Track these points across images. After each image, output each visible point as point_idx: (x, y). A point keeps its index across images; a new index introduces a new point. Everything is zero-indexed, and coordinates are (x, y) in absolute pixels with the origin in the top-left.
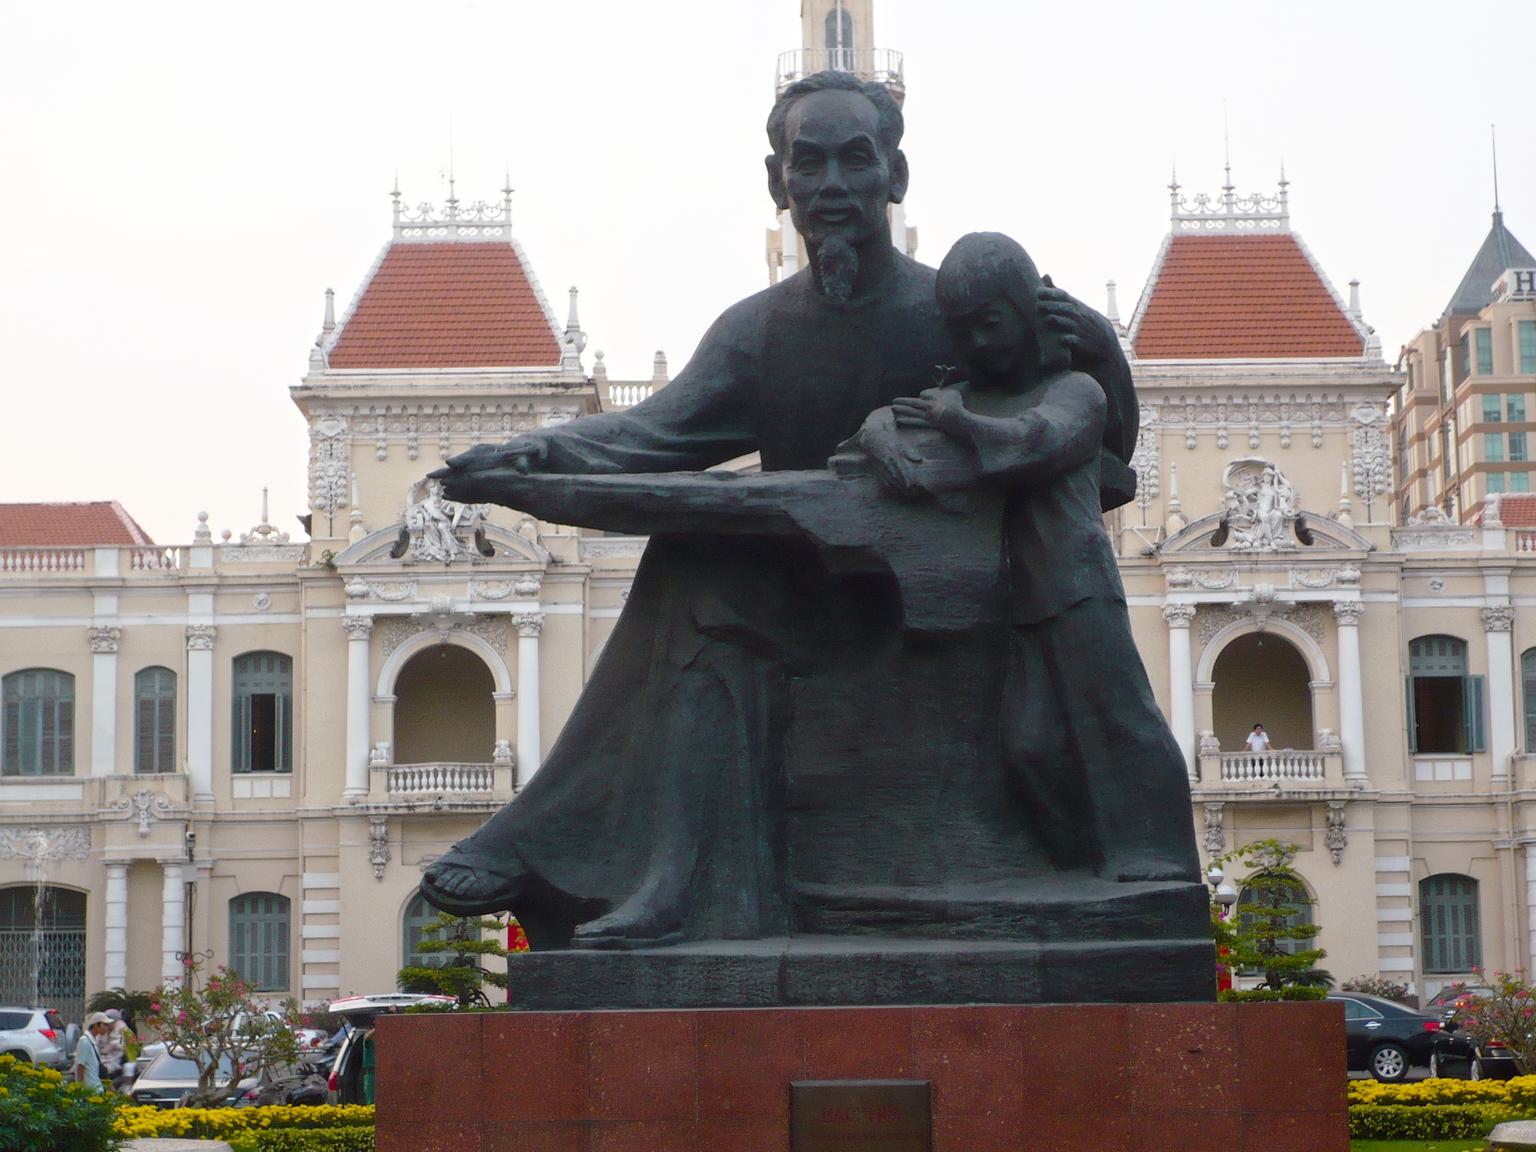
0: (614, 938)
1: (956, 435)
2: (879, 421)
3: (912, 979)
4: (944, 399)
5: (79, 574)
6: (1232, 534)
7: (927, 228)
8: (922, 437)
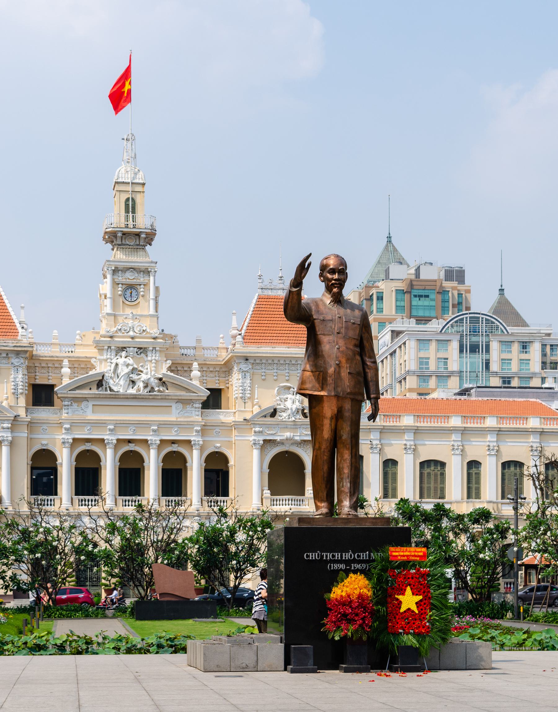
6: (278, 413)
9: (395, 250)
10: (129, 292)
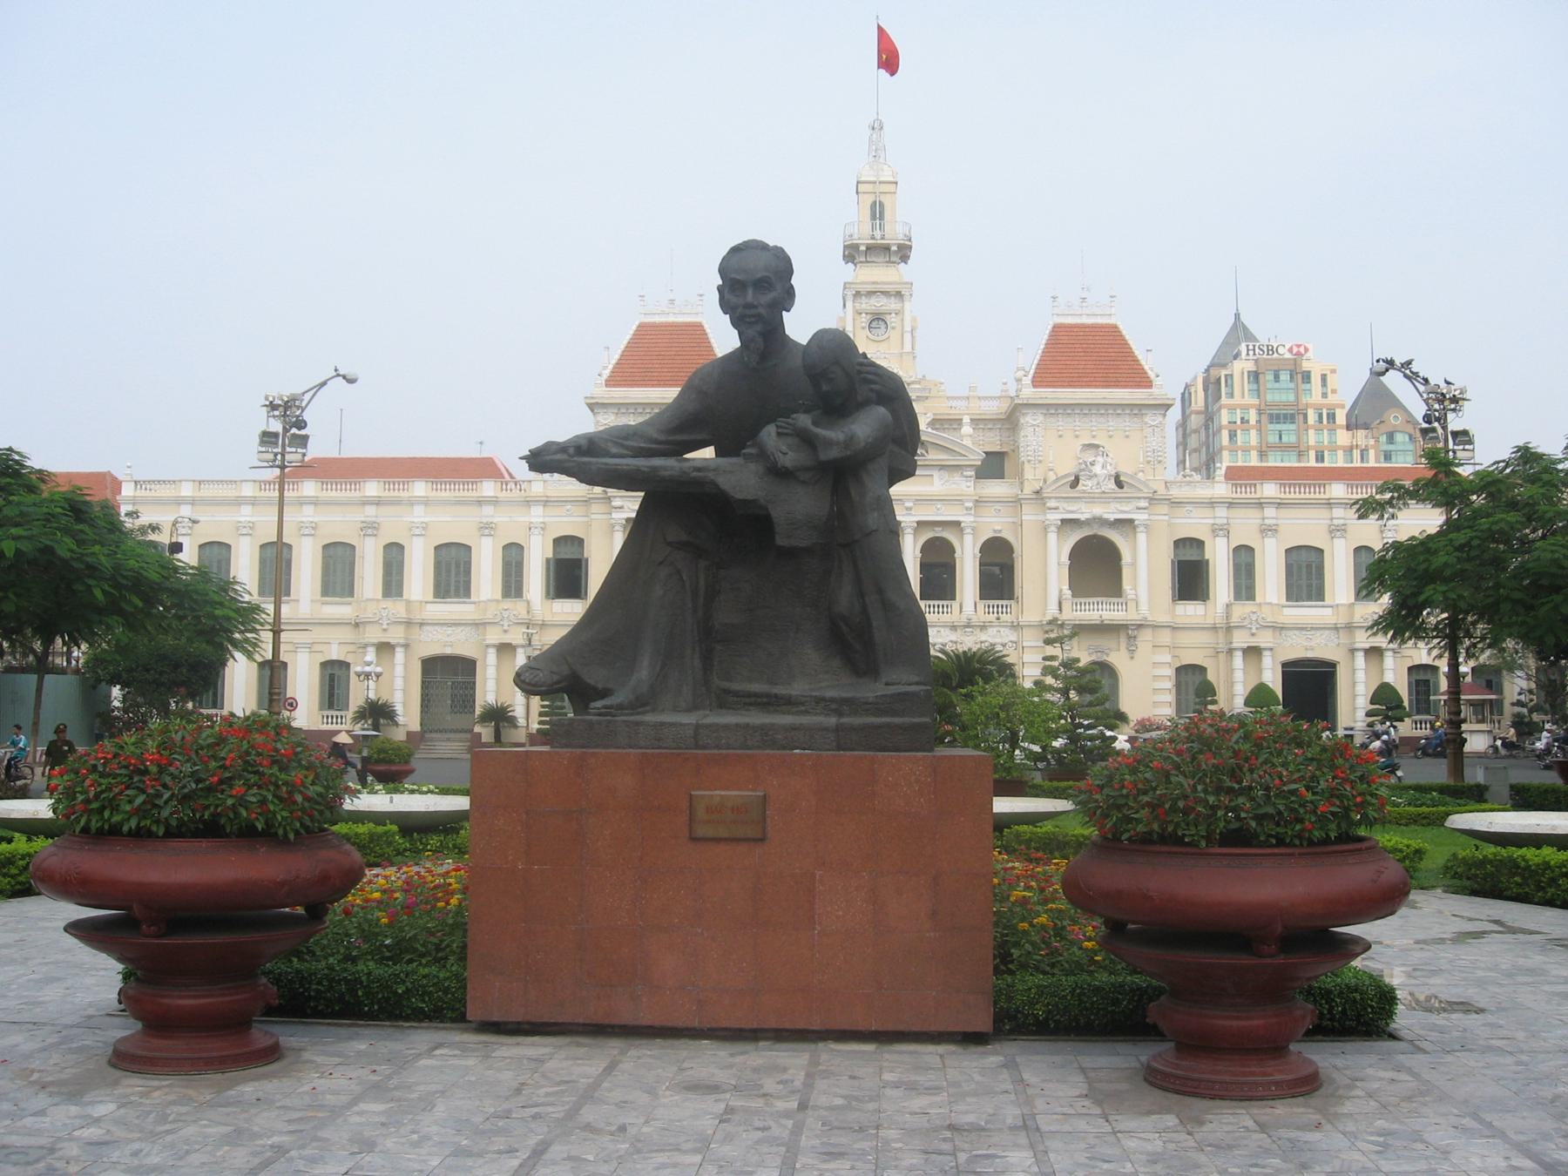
0: (608, 711)
1: (807, 440)
2: (769, 434)
3: (767, 738)
4: (804, 420)
5: (474, 494)
7: (800, 326)
8: (790, 440)
9: (1245, 328)
10: (874, 324)
